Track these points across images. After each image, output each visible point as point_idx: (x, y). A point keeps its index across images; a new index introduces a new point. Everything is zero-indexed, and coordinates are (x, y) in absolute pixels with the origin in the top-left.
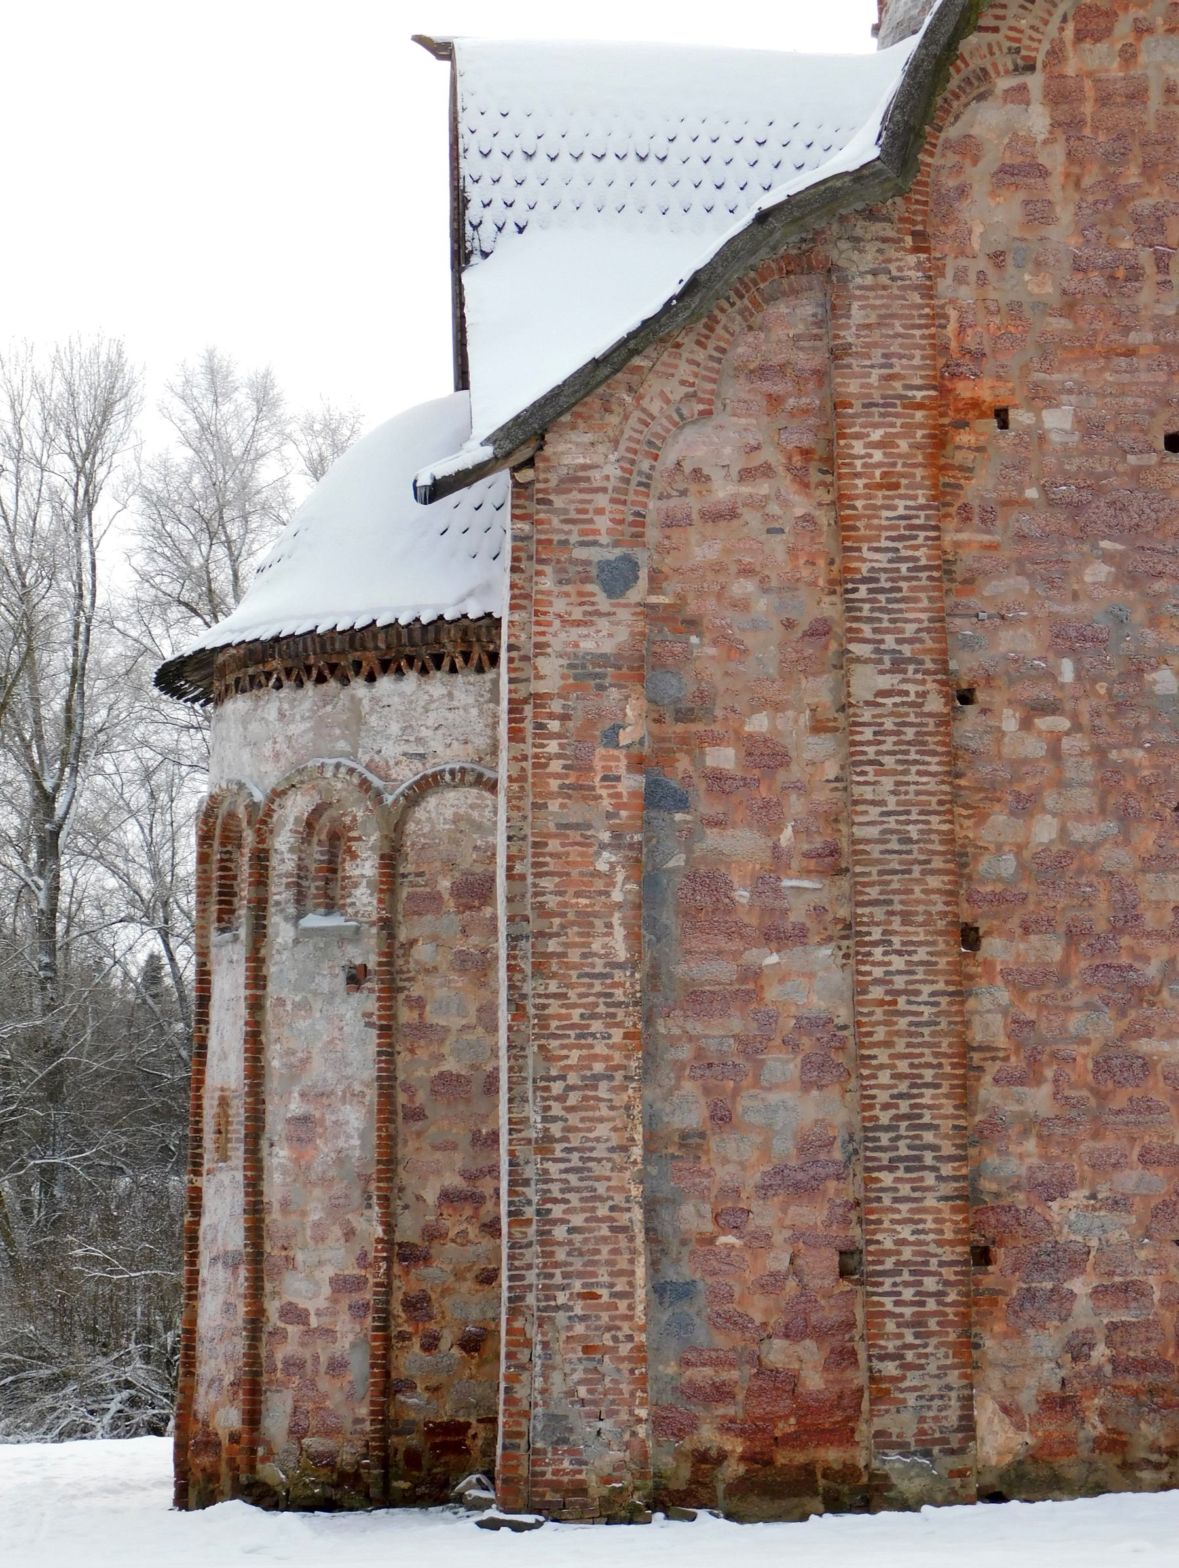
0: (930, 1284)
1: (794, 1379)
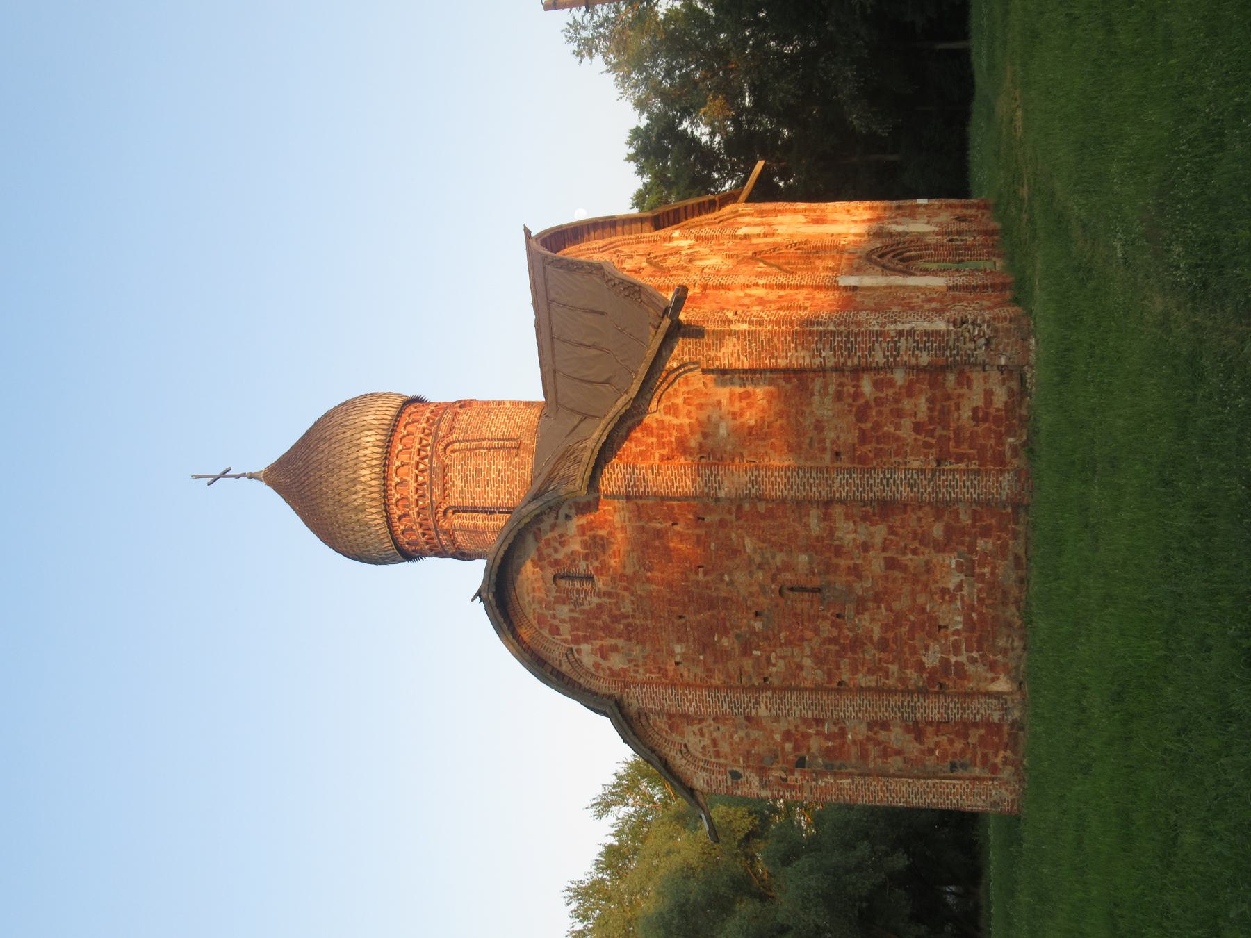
0: (952, 705)
1: (981, 736)
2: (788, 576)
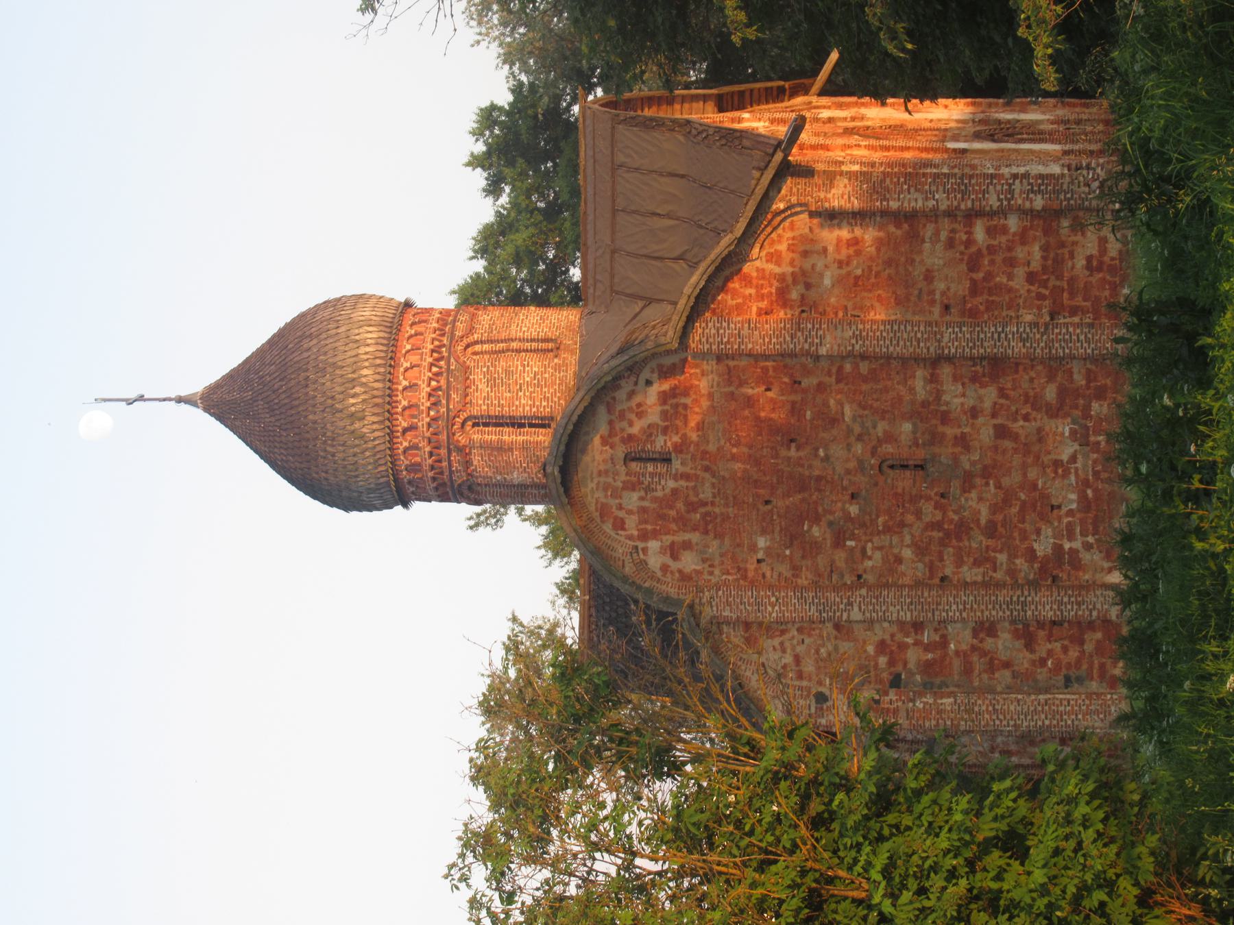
0: (1065, 599)
1: (1098, 642)
2: (889, 449)
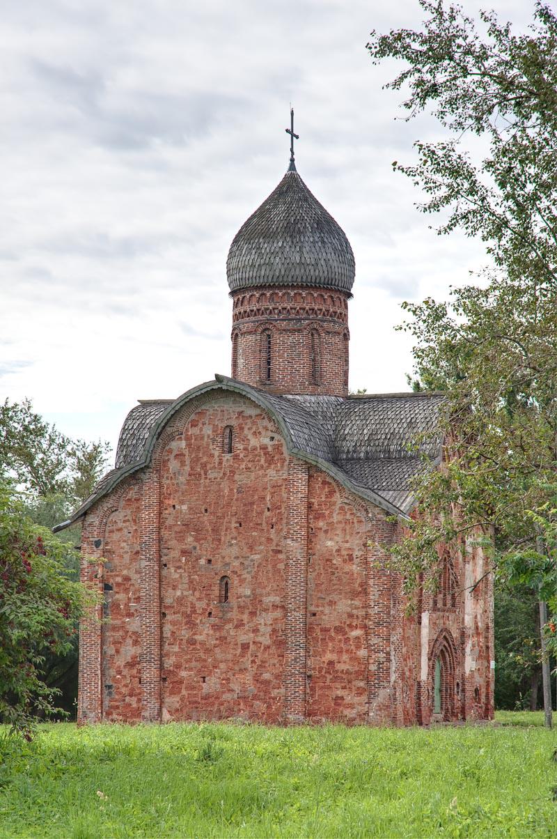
2: (235, 581)
